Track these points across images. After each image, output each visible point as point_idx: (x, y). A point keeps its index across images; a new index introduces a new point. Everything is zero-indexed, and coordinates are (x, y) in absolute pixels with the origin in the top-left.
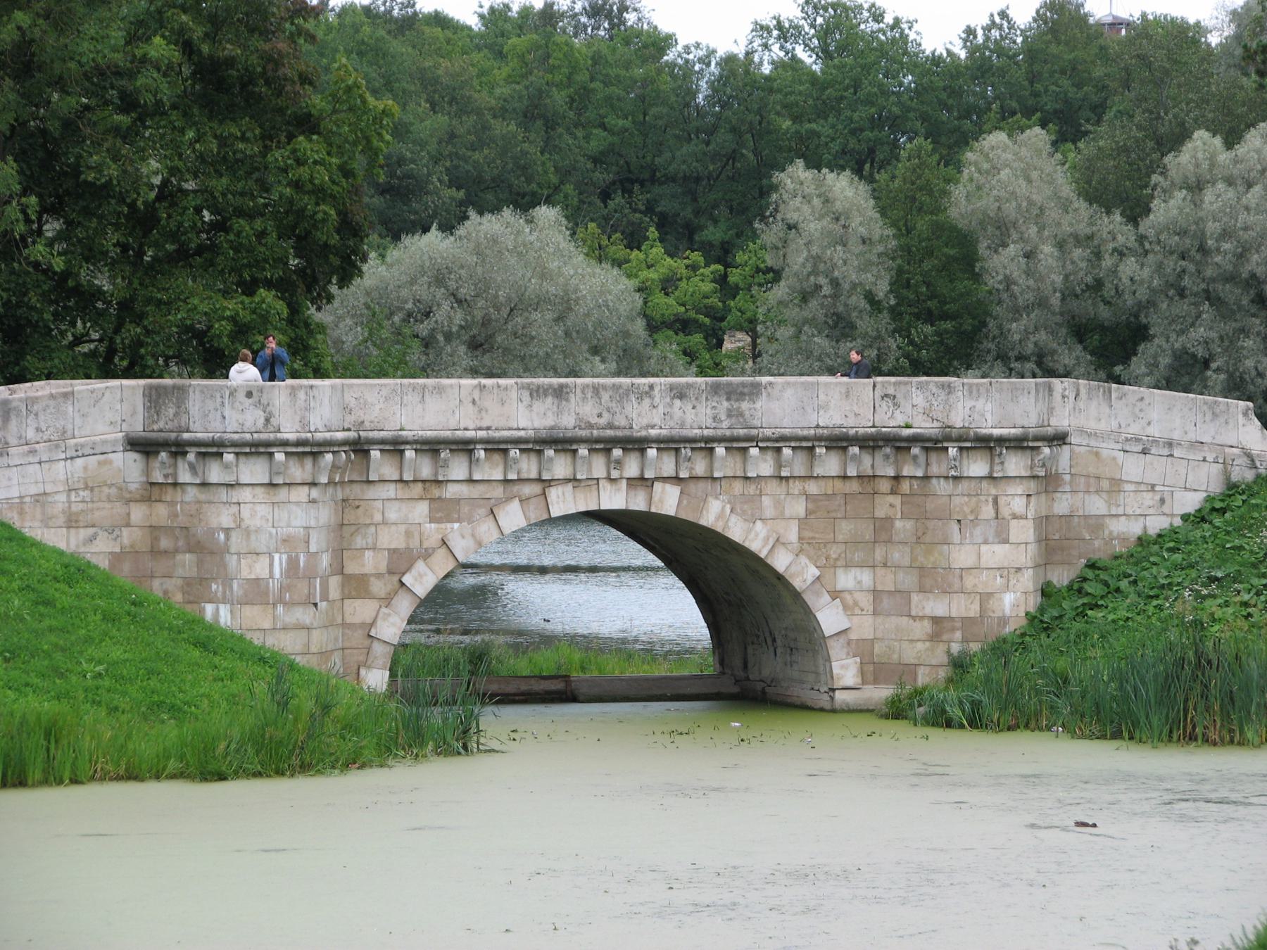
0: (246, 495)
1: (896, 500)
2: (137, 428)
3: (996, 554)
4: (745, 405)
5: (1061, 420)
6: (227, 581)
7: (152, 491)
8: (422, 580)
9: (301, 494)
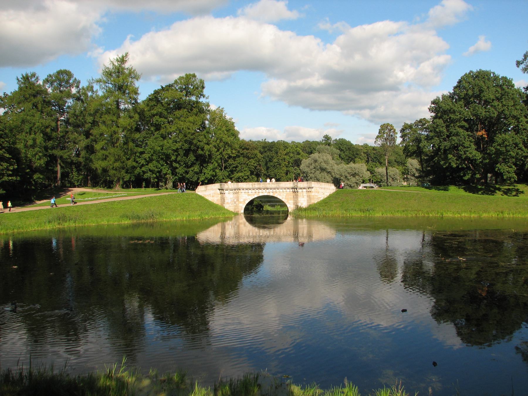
2: (219, 188)
5: (312, 186)
8: (247, 202)
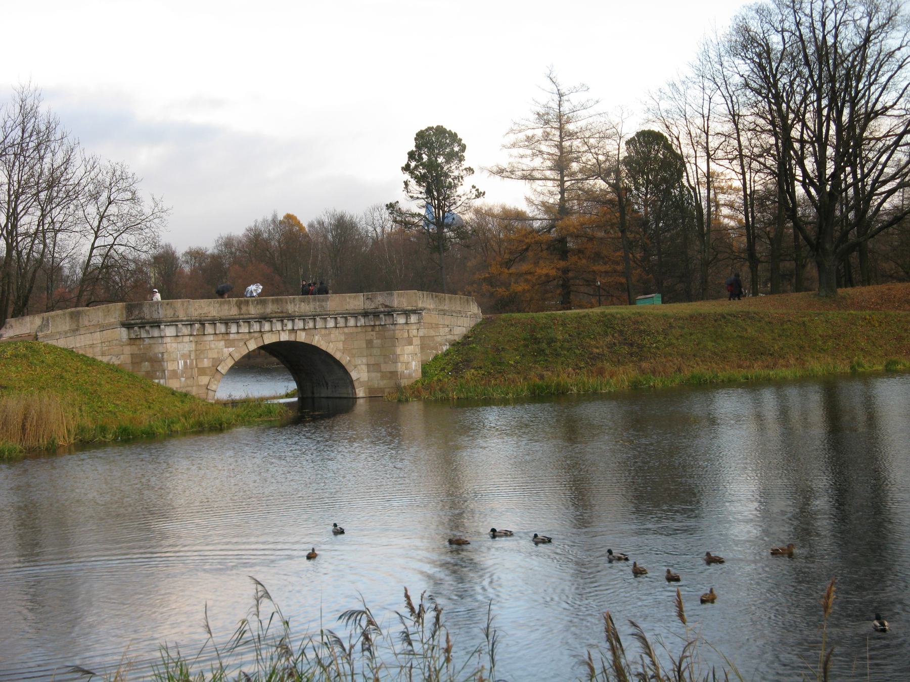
0: (168, 340)
1: (374, 333)
3: (409, 349)
4: (324, 304)
5: (420, 305)
6: (164, 371)
7: (132, 341)
9: (187, 339)
